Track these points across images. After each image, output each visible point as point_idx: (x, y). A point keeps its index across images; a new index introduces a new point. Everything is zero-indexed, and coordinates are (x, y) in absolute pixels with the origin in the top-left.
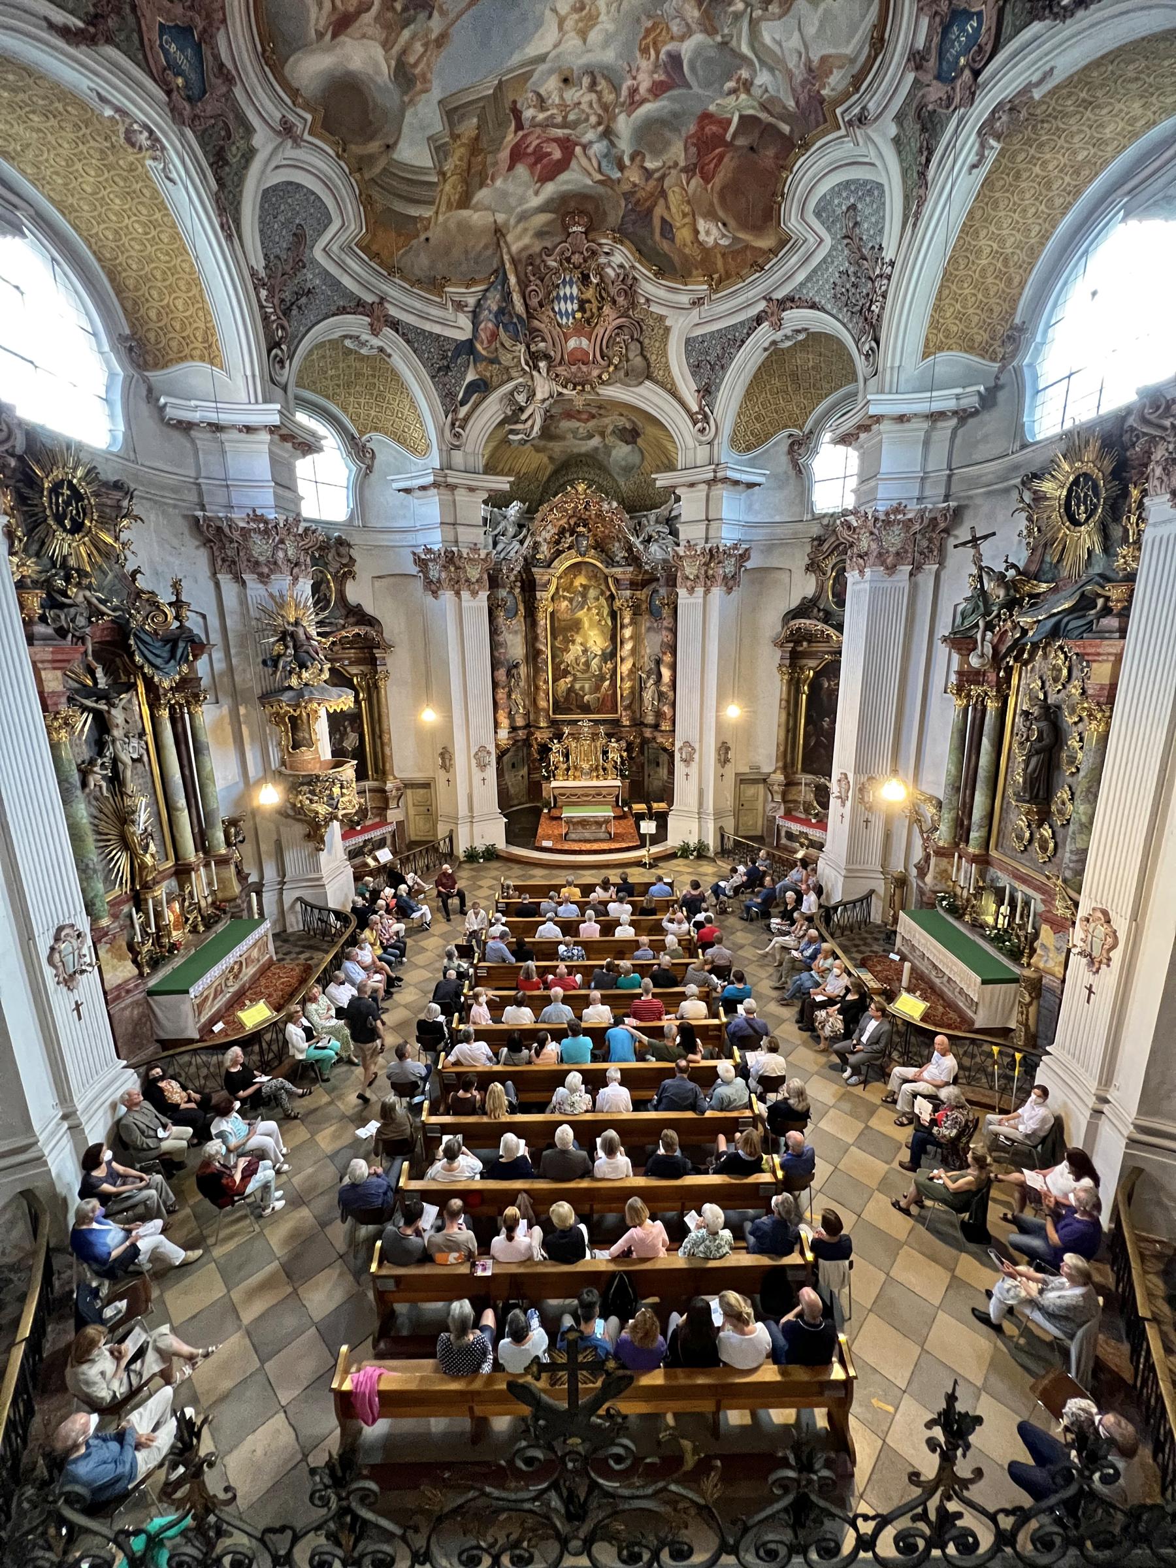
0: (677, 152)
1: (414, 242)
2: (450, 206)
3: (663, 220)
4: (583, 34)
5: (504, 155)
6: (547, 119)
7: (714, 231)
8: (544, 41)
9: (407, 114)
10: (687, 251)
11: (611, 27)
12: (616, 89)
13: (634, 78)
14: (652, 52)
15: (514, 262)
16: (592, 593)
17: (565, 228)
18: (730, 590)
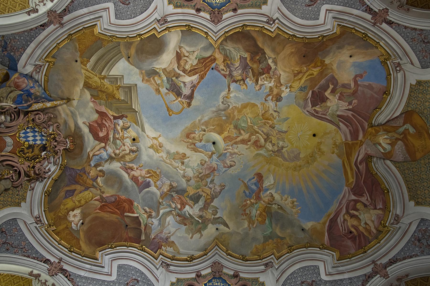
0: (109, 192)
3: (75, 190)
4: (152, 147)
5: (103, 109)
7: (77, 219)
8: (150, 132)
9: (138, 70)
10: (62, 207)
11: (155, 158)
12: (132, 161)
13: (137, 169)
14: (148, 175)
15: (56, 106)
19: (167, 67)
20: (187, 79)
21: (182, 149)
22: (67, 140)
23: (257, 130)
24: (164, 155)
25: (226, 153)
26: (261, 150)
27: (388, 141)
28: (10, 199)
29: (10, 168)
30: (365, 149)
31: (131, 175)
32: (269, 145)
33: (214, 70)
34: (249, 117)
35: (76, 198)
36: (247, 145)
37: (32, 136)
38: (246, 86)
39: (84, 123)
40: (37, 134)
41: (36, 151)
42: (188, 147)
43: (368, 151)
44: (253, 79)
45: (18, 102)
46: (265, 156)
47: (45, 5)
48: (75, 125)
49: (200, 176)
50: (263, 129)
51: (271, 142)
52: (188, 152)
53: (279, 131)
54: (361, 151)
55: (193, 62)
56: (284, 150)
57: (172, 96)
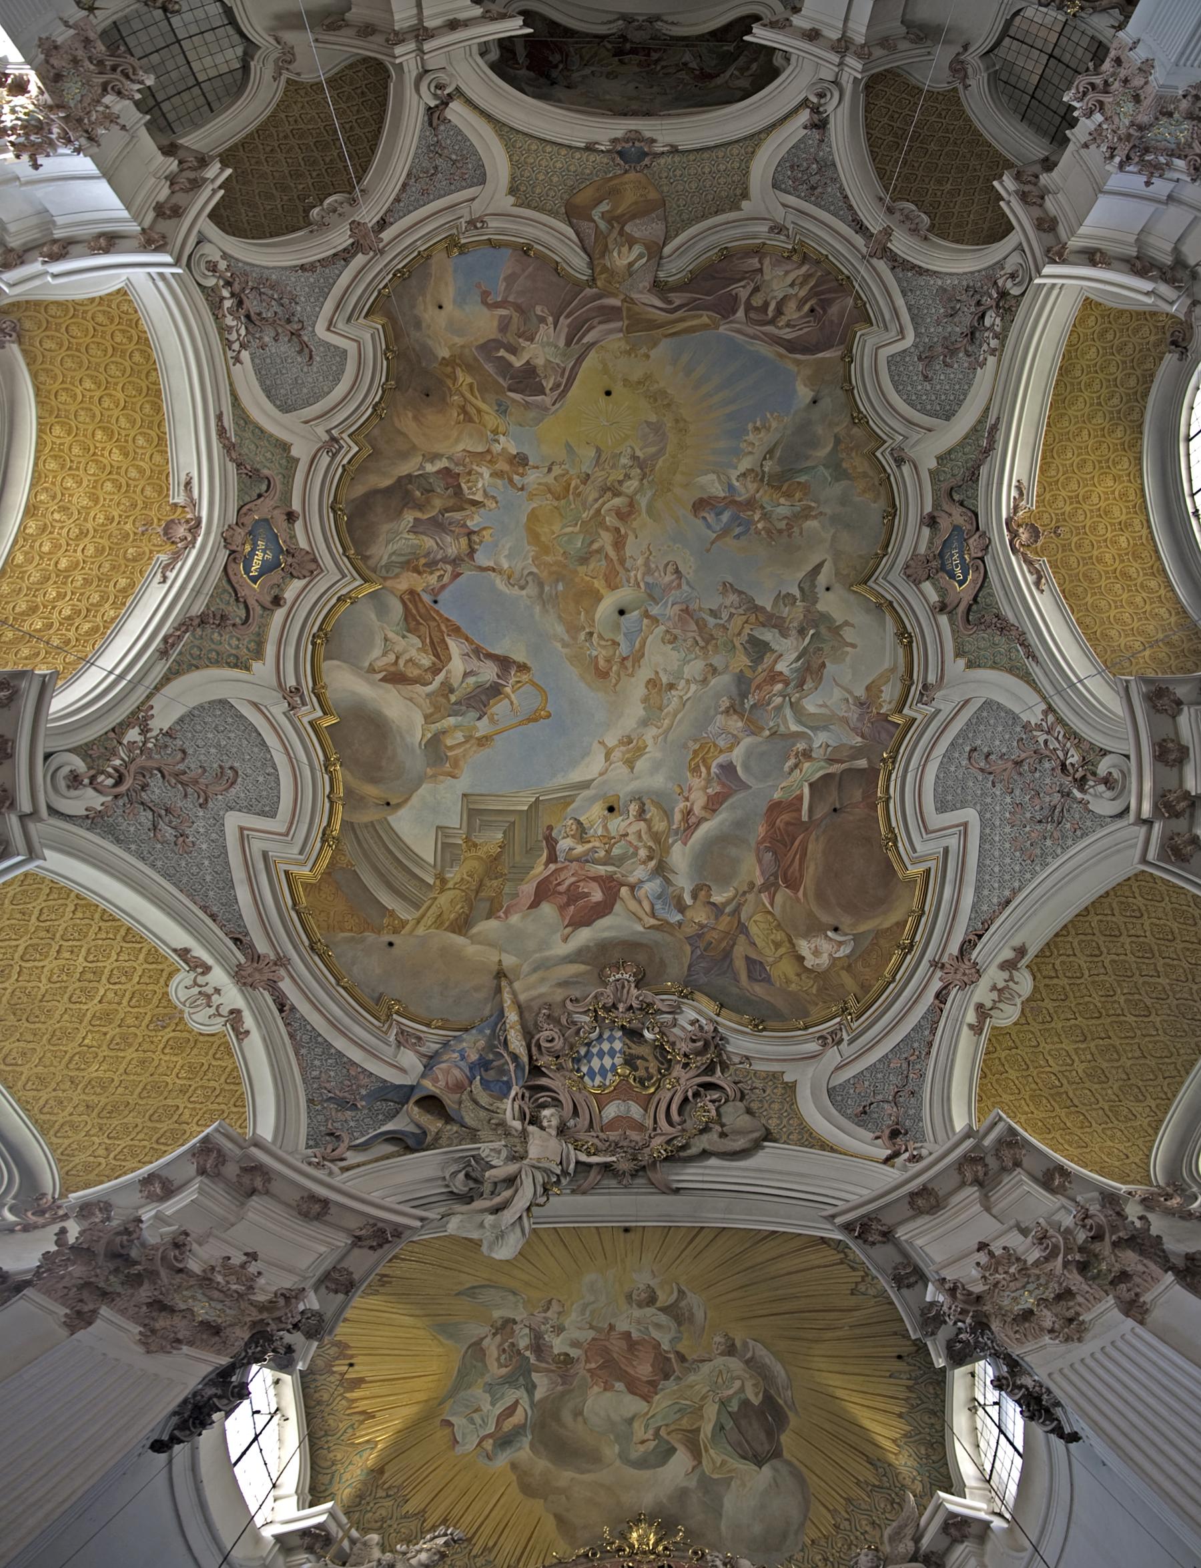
0: (751, 869)
1: (370, 936)
2: (439, 922)
3: (747, 958)
4: (630, 763)
6: (587, 853)
11: (659, 755)
12: (667, 814)
13: (687, 799)
14: (703, 769)
19: (422, 711)
20: (457, 665)
21: (636, 688)
23: (592, 512)
24: (650, 733)
25: (647, 584)
26: (639, 504)
27: (625, 249)
30: (641, 292)
31: (704, 814)
32: (628, 487)
33: (439, 598)
34: (562, 528)
35: (769, 954)
36: (626, 535)
38: (484, 528)
42: (632, 675)
43: (645, 287)
44: (468, 512)
46: (654, 495)
49: (702, 643)
50: (591, 499)
51: (621, 483)
52: (644, 673)
53: (597, 464)
54: (646, 301)
55: (413, 645)
56: (638, 453)
57: (499, 708)
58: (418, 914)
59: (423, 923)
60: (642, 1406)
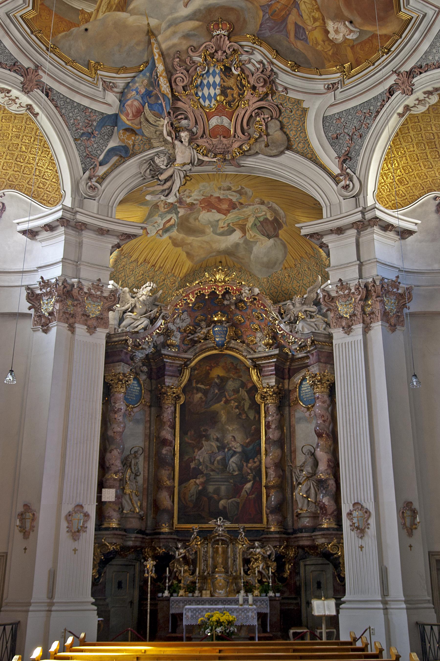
3: (296, 24)
7: (343, 29)
10: (319, 48)
15: (162, 54)
16: (231, 385)
17: (209, 32)
18: (393, 328)
22: (215, 34)
28: (296, 123)
29: (252, 120)
35: (310, 24)
37: (209, 89)
39: (186, 5)
40: (205, 82)
41: (231, 82)
45: (160, 109)
47: (17, 98)
48: (190, 19)
58: (96, 6)
59: (100, 11)
60: (223, 217)
